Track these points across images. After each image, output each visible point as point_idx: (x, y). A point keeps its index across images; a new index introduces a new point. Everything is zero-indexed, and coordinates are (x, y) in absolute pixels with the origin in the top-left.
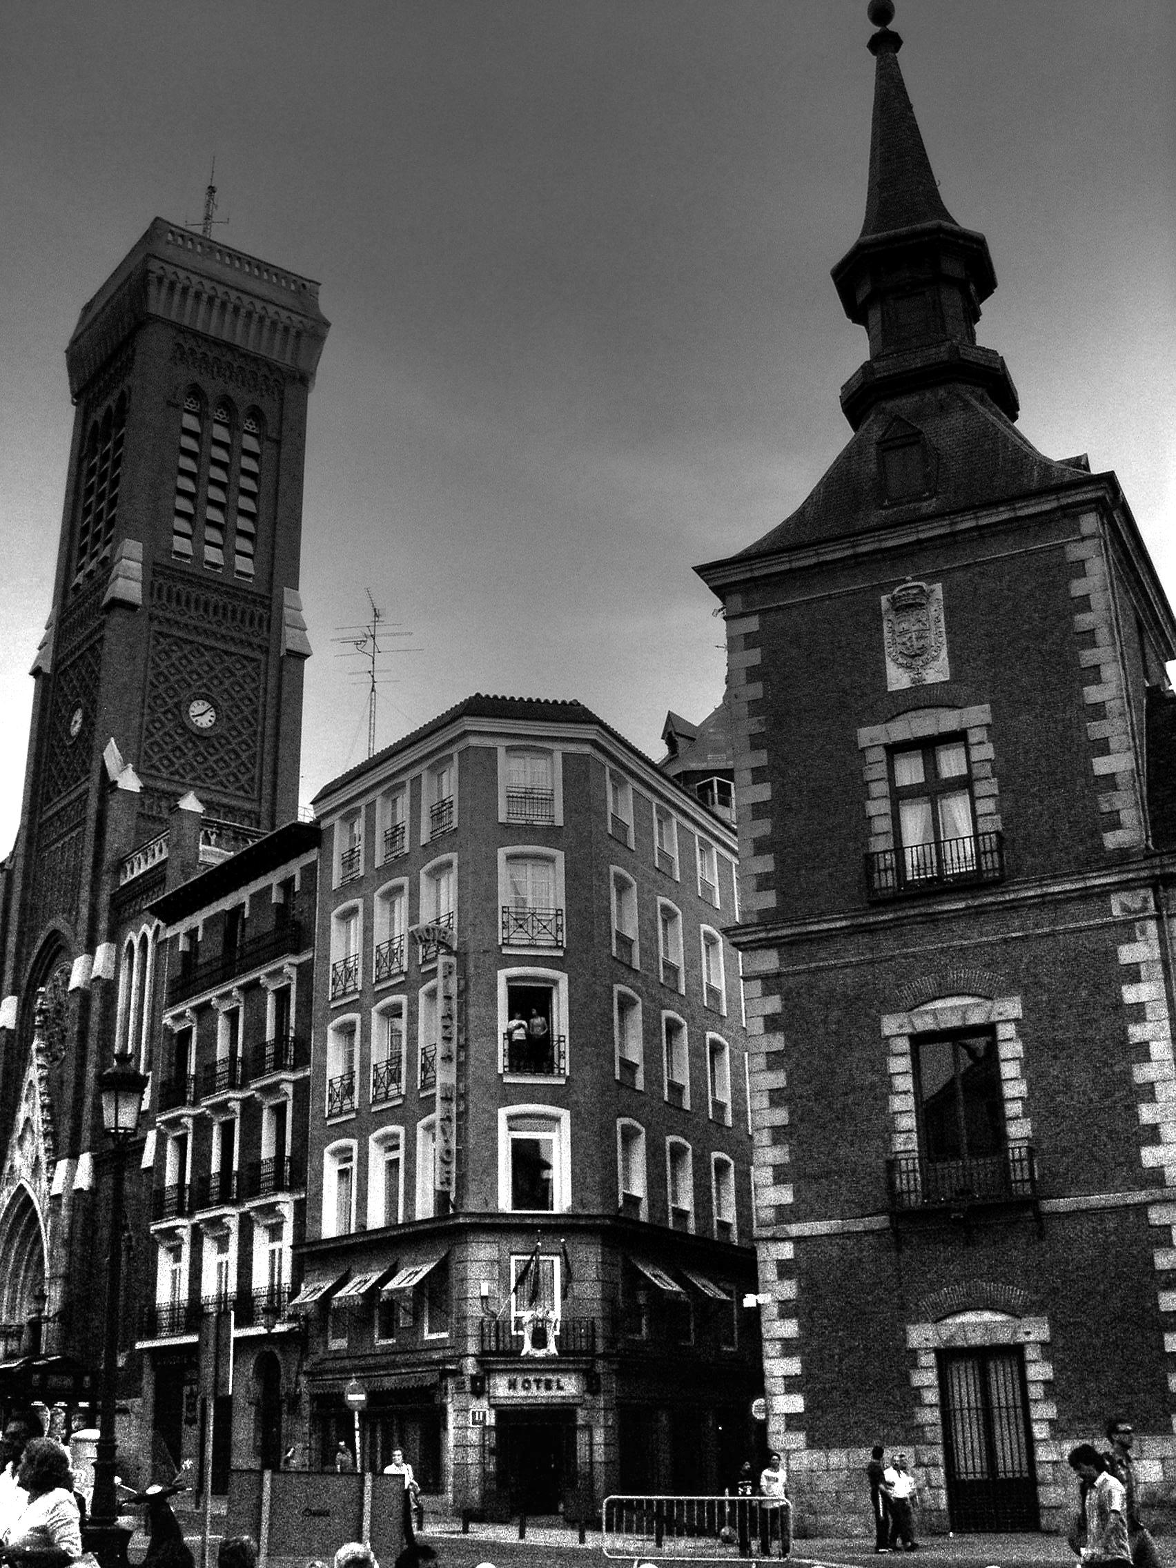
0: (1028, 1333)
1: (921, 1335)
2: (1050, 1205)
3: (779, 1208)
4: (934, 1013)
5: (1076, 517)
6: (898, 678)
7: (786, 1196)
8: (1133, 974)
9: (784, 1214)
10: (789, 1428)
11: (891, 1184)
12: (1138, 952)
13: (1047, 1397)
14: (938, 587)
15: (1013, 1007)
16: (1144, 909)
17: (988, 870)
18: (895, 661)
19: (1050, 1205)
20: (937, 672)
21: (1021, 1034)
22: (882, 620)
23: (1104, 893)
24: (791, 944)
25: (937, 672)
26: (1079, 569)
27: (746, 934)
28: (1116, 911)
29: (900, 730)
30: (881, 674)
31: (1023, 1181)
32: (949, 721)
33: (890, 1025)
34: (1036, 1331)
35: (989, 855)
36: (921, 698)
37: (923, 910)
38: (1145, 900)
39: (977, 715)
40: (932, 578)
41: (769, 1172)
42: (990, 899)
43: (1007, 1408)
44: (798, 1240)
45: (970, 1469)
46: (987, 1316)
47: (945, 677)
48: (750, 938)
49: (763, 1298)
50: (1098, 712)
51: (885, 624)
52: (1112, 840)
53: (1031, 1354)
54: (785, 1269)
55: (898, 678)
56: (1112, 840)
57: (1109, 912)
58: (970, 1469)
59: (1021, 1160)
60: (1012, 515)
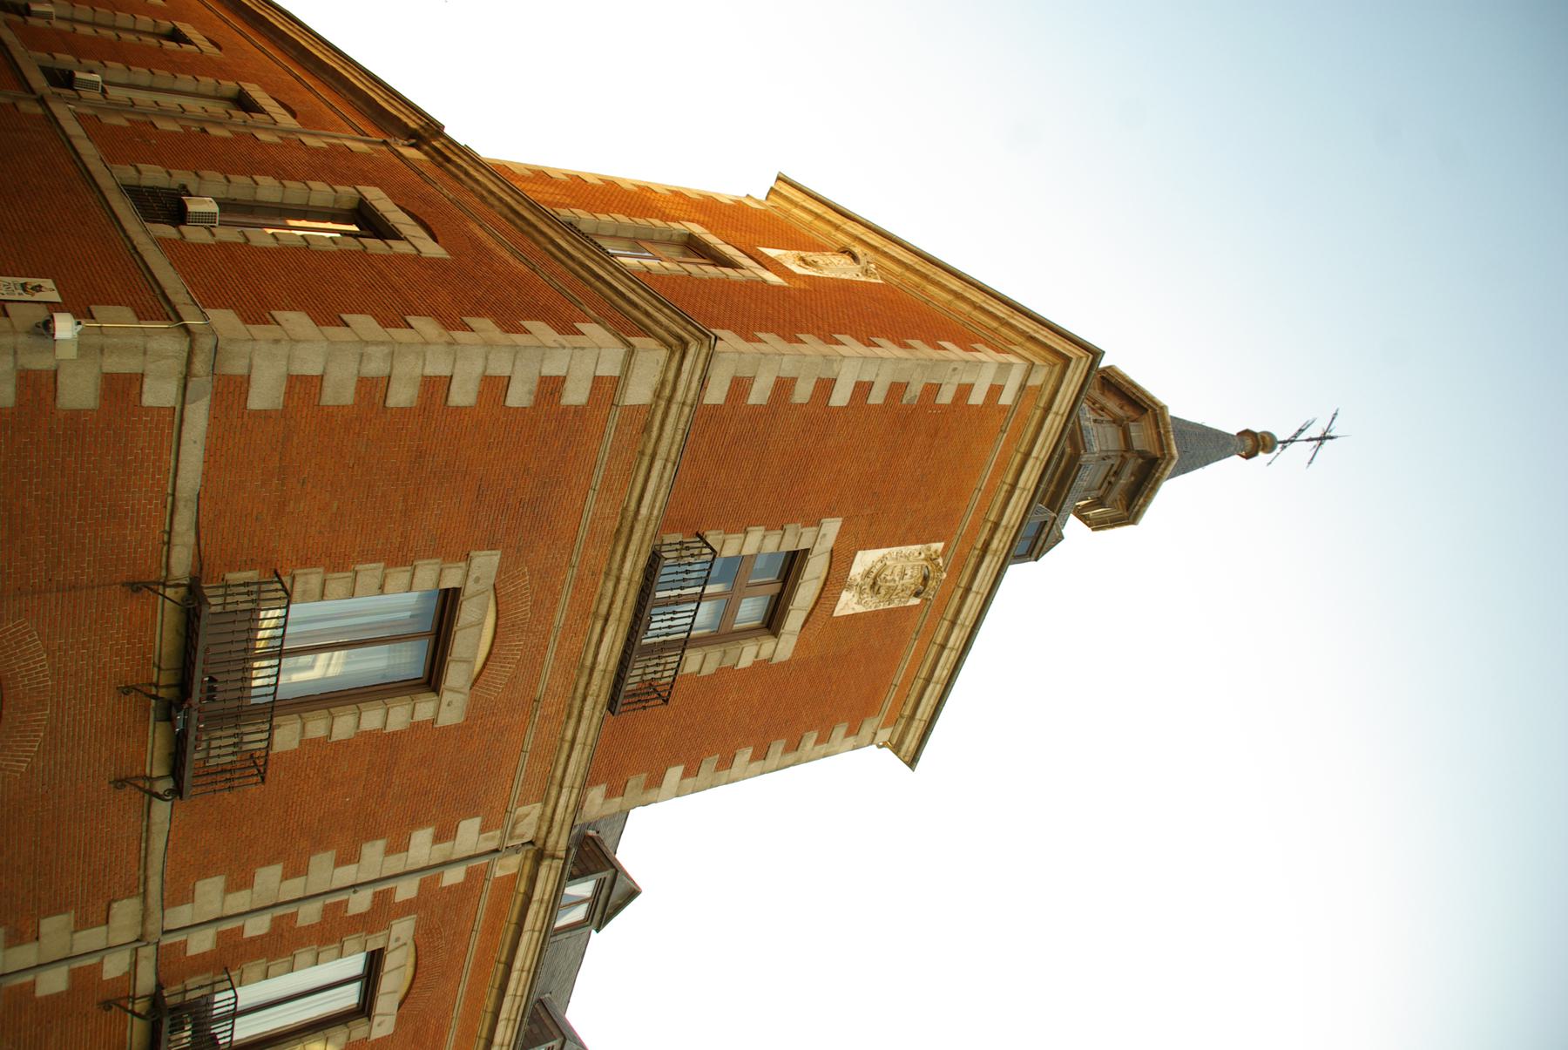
7: (265, 394)
24: (647, 428)
37: (616, 610)
38: (522, 836)
41: (312, 368)
42: (594, 688)
44: (175, 418)
48: (684, 376)
49: (67, 353)
51: (918, 547)
54: (121, 390)
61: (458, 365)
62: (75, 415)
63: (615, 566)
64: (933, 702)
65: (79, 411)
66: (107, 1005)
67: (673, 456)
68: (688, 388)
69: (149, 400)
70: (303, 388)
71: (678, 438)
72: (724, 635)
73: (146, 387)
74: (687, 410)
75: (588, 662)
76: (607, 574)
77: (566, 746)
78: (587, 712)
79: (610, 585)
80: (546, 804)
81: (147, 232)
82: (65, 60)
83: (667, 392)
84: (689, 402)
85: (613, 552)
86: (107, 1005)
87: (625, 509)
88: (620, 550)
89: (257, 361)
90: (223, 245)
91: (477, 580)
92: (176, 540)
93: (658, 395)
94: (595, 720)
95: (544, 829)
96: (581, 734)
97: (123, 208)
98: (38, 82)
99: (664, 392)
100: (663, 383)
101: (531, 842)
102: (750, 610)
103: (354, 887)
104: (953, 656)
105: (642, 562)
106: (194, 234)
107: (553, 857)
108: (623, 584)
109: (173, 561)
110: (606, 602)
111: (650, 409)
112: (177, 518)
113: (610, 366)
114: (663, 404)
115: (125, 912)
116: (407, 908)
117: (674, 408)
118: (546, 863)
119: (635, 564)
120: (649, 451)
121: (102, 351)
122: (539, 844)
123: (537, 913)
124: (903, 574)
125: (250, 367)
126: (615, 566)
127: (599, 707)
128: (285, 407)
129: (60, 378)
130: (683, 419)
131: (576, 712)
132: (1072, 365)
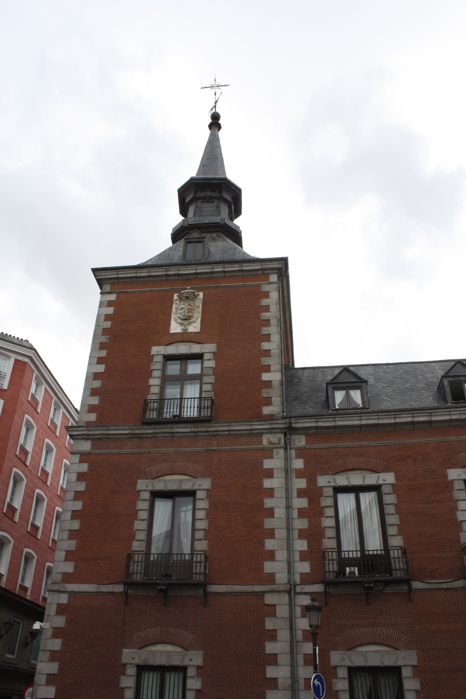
0: (191, 660)
1: (131, 656)
2: (213, 588)
4: (165, 481)
5: (268, 275)
7: (69, 567)
8: (270, 474)
9: (67, 578)
11: (128, 567)
12: (274, 463)
14: (201, 295)
15: (206, 483)
16: (279, 443)
18: (176, 320)
19: (213, 588)
20: (195, 327)
21: (208, 497)
23: (260, 434)
24: (100, 439)
25: (195, 327)
26: (266, 295)
27: (77, 431)
28: (265, 442)
29: (172, 350)
30: (169, 324)
31: (200, 574)
32: (196, 349)
33: (141, 484)
34: (195, 659)
35: (206, 407)
36: (185, 338)
37: (168, 430)
38: (280, 439)
40: (199, 290)
42: (203, 429)
44: (72, 594)
46: (169, 648)
47: (198, 330)
48: (79, 433)
49: (46, 625)
50: (267, 353)
51: (174, 306)
52: (266, 410)
53: (191, 672)
55: (175, 328)
56: (266, 410)
57: (261, 443)
59: (200, 562)
60: (240, 268)
61: (68, 509)
62: (67, 622)
63: (151, 436)
65: (66, 621)
67: (106, 428)
68: (83, 430)
69: (65, 602)
71: (100, 428)
73: (62, 603)
74: (90, 429)
75: (193, 434)
76: (155, 437)
77: (232, 433)
78: (214, 429)
79: (159, 435)
83: (86, 437)
84: (87, 429)
85: (146, 438)
87: (129, 438)
88: (144, 436)
89: (58, 571)
91: (147, 486)
92: (111, 590)
93: (88, 439)
94: (217, 425)
95: (275, 431)
103: (288, 507)
105: (147, 427)
108: (157, 431)
109: (118, 591)
110: (166, 435)
111: (93, 440)
112: (104, 591)
114: (90, 437)
115: (269, 599)
116: (312, 481)
117: (90, 433)
118: (294, 425)
119: (148, 429)
120: (107, 436)
121: (49, 616)
123: (324, 422)
124: (182, 309)
125: (60, 573)
126: (151, 436)
127: (211, 425)
128: (74, 561)
129: (56, 626)
130: (93, 429)
131: (215, 433)
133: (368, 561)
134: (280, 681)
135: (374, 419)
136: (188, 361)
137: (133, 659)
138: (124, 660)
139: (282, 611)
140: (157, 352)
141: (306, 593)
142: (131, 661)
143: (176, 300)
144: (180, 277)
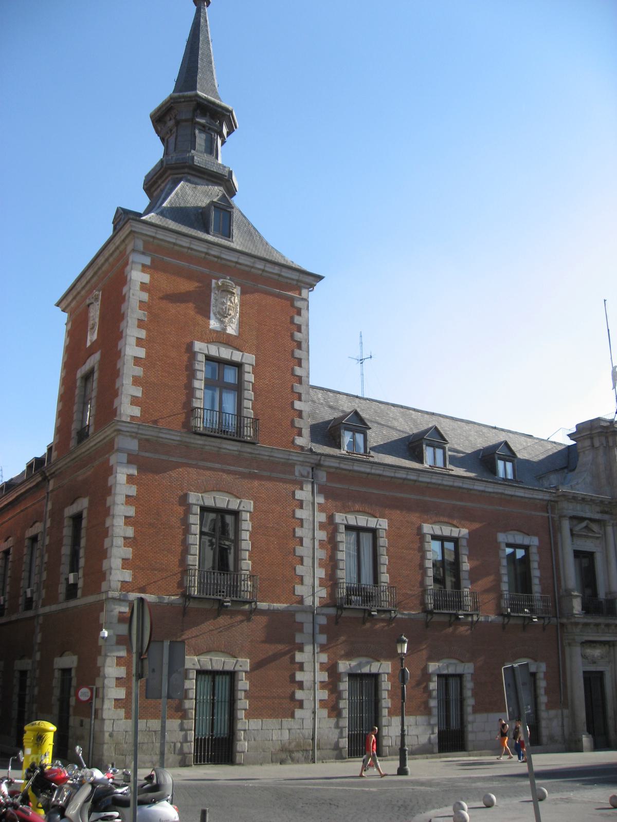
3: (124, 583)
6: (214, 324)
7: (127, 576)
10: (116, 707)
13: (246, 698)
17: (247, 436)
18: (215, 314)
22: (211, 292)
24: (147, 440)
38: (308, 473)
39: (249, 359)
43: (221, 702)
45: (222, 732)
51: (212, 294)
58: (222, 732)
61: (121, 514)
64: (290, 272)
66: (337, 623)
70: (126, 564)
72: (238, 388)
78: (257, 452)
80: (295, 464)
81: (79, 598)
82: (21, 600)
83: (134, 434)
86: (337, 623)
90: (84, 576)
93: (135, 438)
95: (307, 464)
96: (266, 454)
97: (72, 603)
98: (30, 614)
99: (134, 435)
100: (131, 436)
101: (313, 468)
102: (230, 376)
104: (268, 265)
106: (81, 584)
107: (320, 460)
108: (206, 443)
111: (140, 440)
113: (124, 457)
117: (140, 432)
119: (199, 440)
121: (111, 623)
122: (313, 466)
123: (345, 464)
132: (134, 229)
133: (367, 593)
134: (305, 684)
135: (381, 470)
136: (226, 366)
137: (194, 664)
138: (188, 665)
139: (308, 628)
140: (200, 349)
141: (323, 614)
142: (192, 667)
143: (214, 288)
144: (219, 260)
